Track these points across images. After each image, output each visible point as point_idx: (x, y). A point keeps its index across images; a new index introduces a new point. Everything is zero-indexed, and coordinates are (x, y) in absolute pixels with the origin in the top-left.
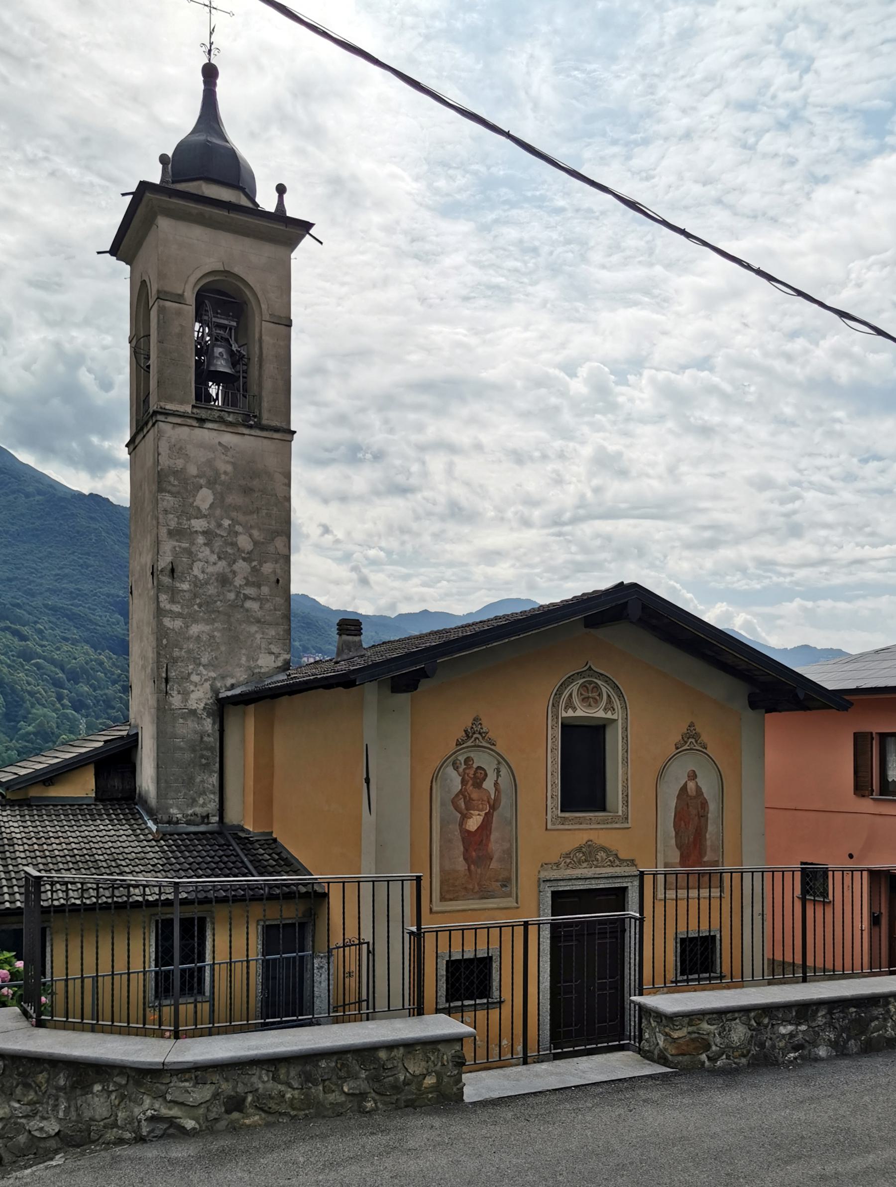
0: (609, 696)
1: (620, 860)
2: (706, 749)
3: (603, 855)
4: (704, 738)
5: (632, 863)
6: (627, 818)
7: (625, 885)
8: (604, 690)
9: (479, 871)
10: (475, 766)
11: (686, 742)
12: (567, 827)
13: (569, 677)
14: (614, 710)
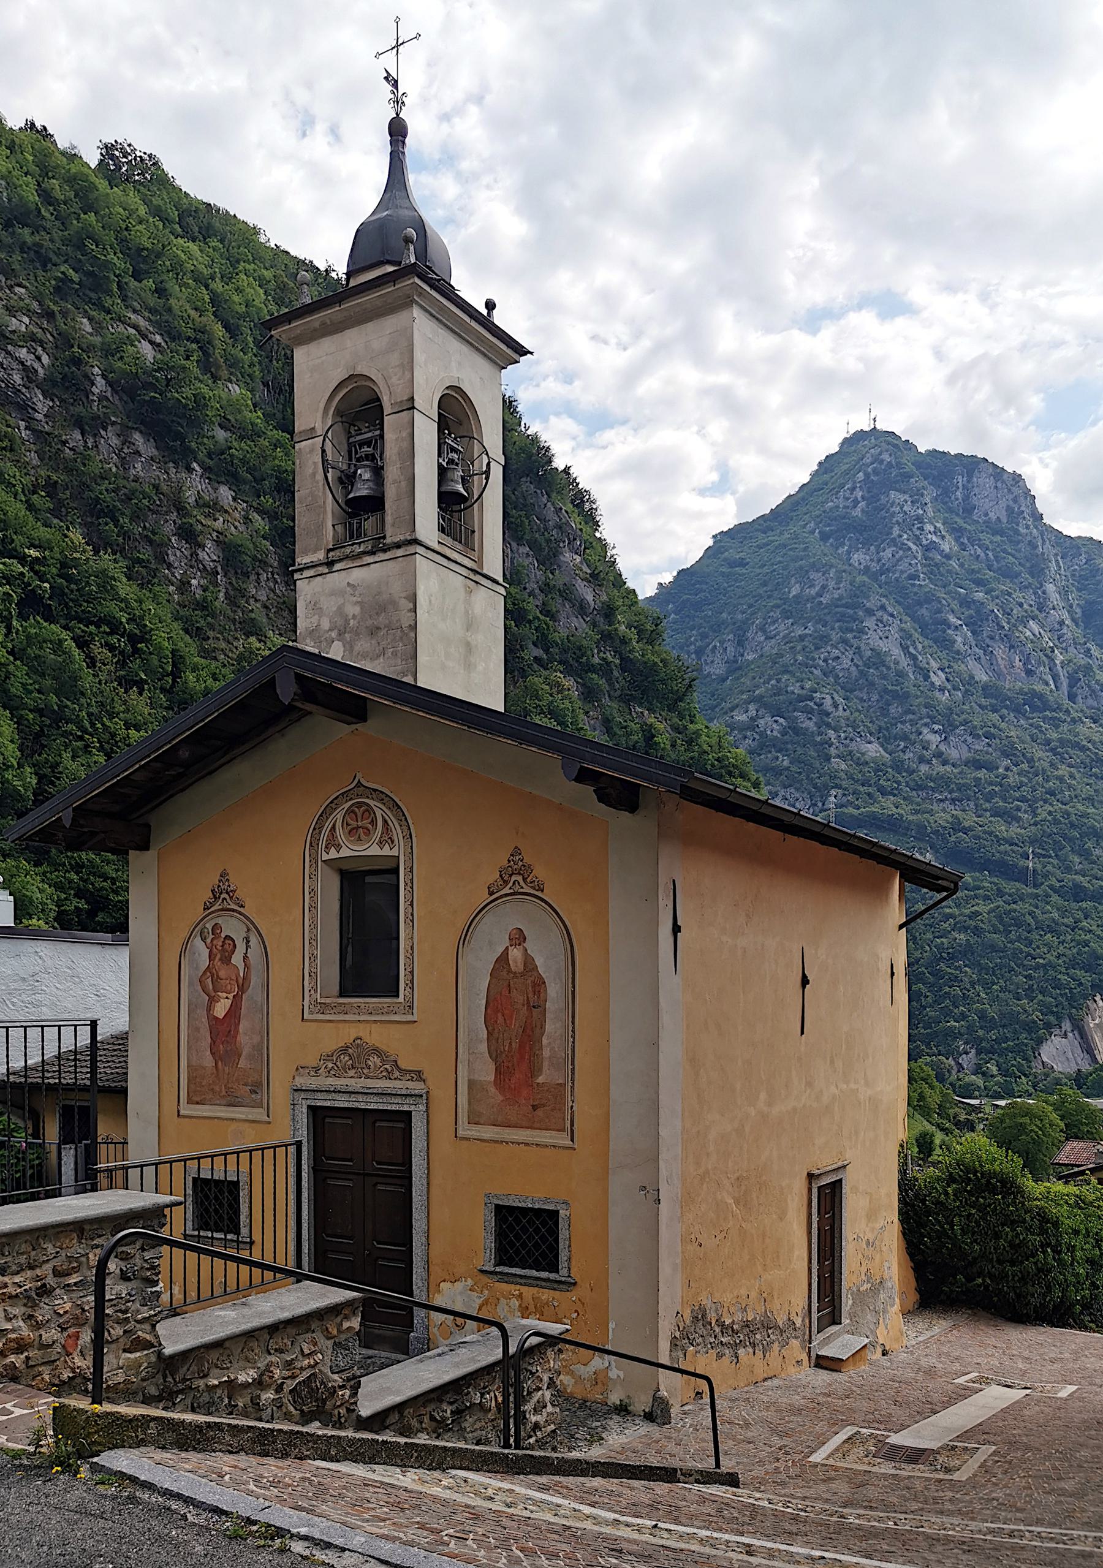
0: (385, 821)
1: (400, 1070)
2: (542, 891)
3: (378, 1061)
4: (540, 872)
5: (418, 1076)
6: (411, 1007)
7: (406, 1108)
8: (379, 813)
9: (226, 1069)
10: (223, 935)
11: (506, 883)
12: (328, 1017)
13: (332, 802)
14: (393, 842)
